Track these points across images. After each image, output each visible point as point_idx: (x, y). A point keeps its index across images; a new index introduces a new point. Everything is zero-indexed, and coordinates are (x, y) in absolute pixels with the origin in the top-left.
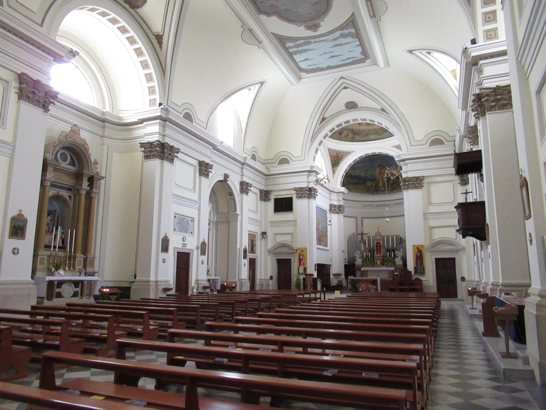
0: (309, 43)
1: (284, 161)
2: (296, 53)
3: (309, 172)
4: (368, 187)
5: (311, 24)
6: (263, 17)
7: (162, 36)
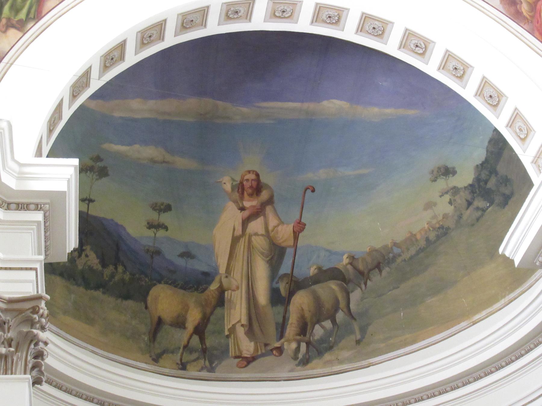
4: (160, 322)
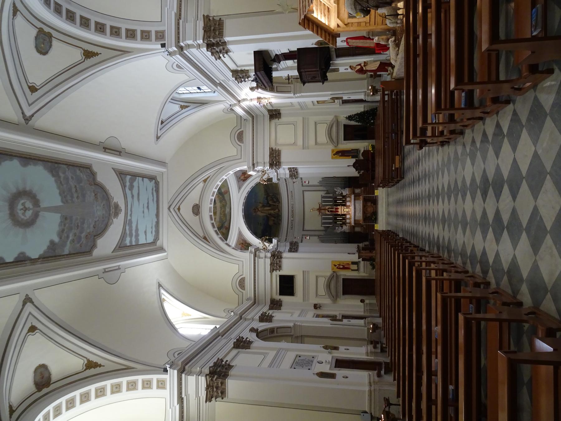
0: (131, 222)
1: (242, 283)
2: (137, 240)
3: (255, 256)
5: (113, 210)
6: (96, 253)
7: (88, 360)
